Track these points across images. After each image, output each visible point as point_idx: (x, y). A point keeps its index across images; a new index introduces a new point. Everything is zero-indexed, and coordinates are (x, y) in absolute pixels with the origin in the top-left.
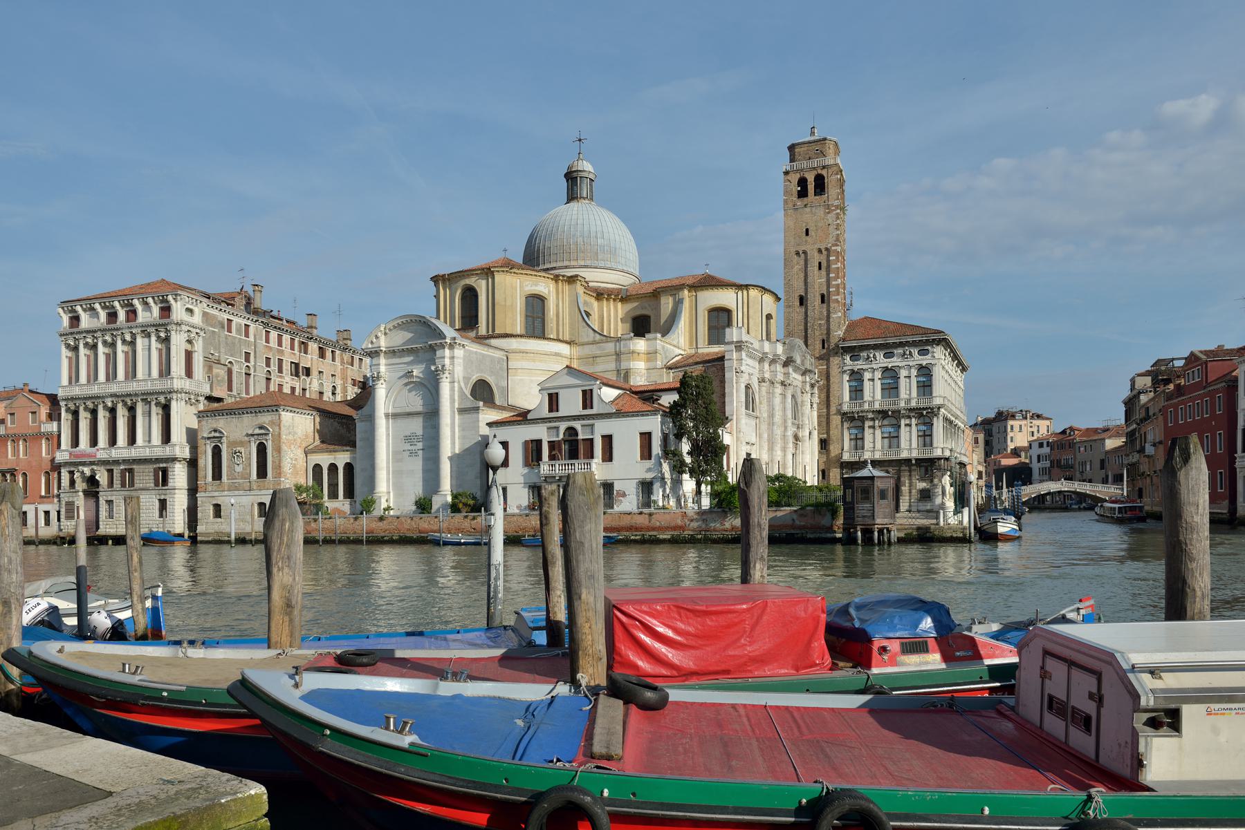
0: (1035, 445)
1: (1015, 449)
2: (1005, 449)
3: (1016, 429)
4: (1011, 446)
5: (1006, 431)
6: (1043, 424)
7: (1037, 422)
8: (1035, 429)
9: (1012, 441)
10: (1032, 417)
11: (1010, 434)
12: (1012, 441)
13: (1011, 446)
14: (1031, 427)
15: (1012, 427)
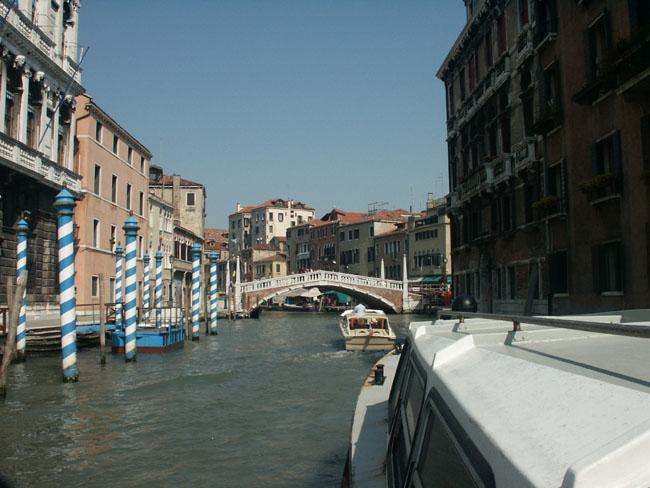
0: (294, 234)
1: (274, 239)
2: (264, 240)
3: (275, 216)
4: (270, 237)
5: (264, 221)
6: (305, 215)
7: (299, 212)
8: (295, 219)
9: (271, 231)
10: (294, 206)
11: (270, 223)
12: (271, 231)
13: (270, 237)
14: (292, 216)
15: (271, 214)
